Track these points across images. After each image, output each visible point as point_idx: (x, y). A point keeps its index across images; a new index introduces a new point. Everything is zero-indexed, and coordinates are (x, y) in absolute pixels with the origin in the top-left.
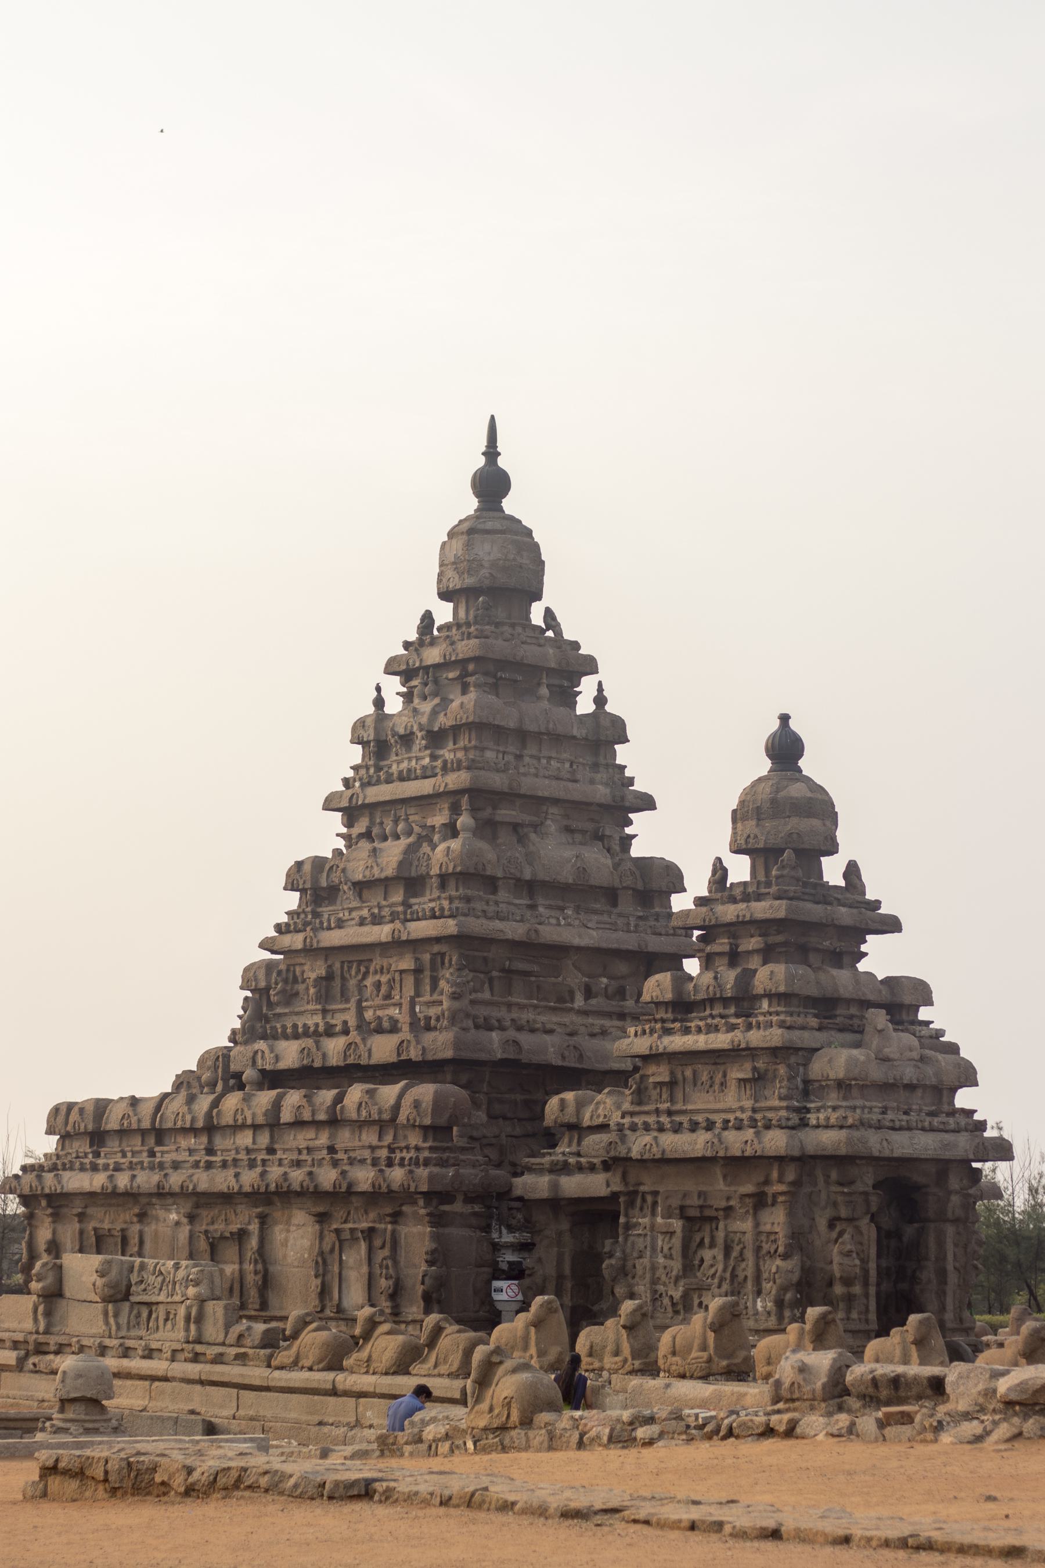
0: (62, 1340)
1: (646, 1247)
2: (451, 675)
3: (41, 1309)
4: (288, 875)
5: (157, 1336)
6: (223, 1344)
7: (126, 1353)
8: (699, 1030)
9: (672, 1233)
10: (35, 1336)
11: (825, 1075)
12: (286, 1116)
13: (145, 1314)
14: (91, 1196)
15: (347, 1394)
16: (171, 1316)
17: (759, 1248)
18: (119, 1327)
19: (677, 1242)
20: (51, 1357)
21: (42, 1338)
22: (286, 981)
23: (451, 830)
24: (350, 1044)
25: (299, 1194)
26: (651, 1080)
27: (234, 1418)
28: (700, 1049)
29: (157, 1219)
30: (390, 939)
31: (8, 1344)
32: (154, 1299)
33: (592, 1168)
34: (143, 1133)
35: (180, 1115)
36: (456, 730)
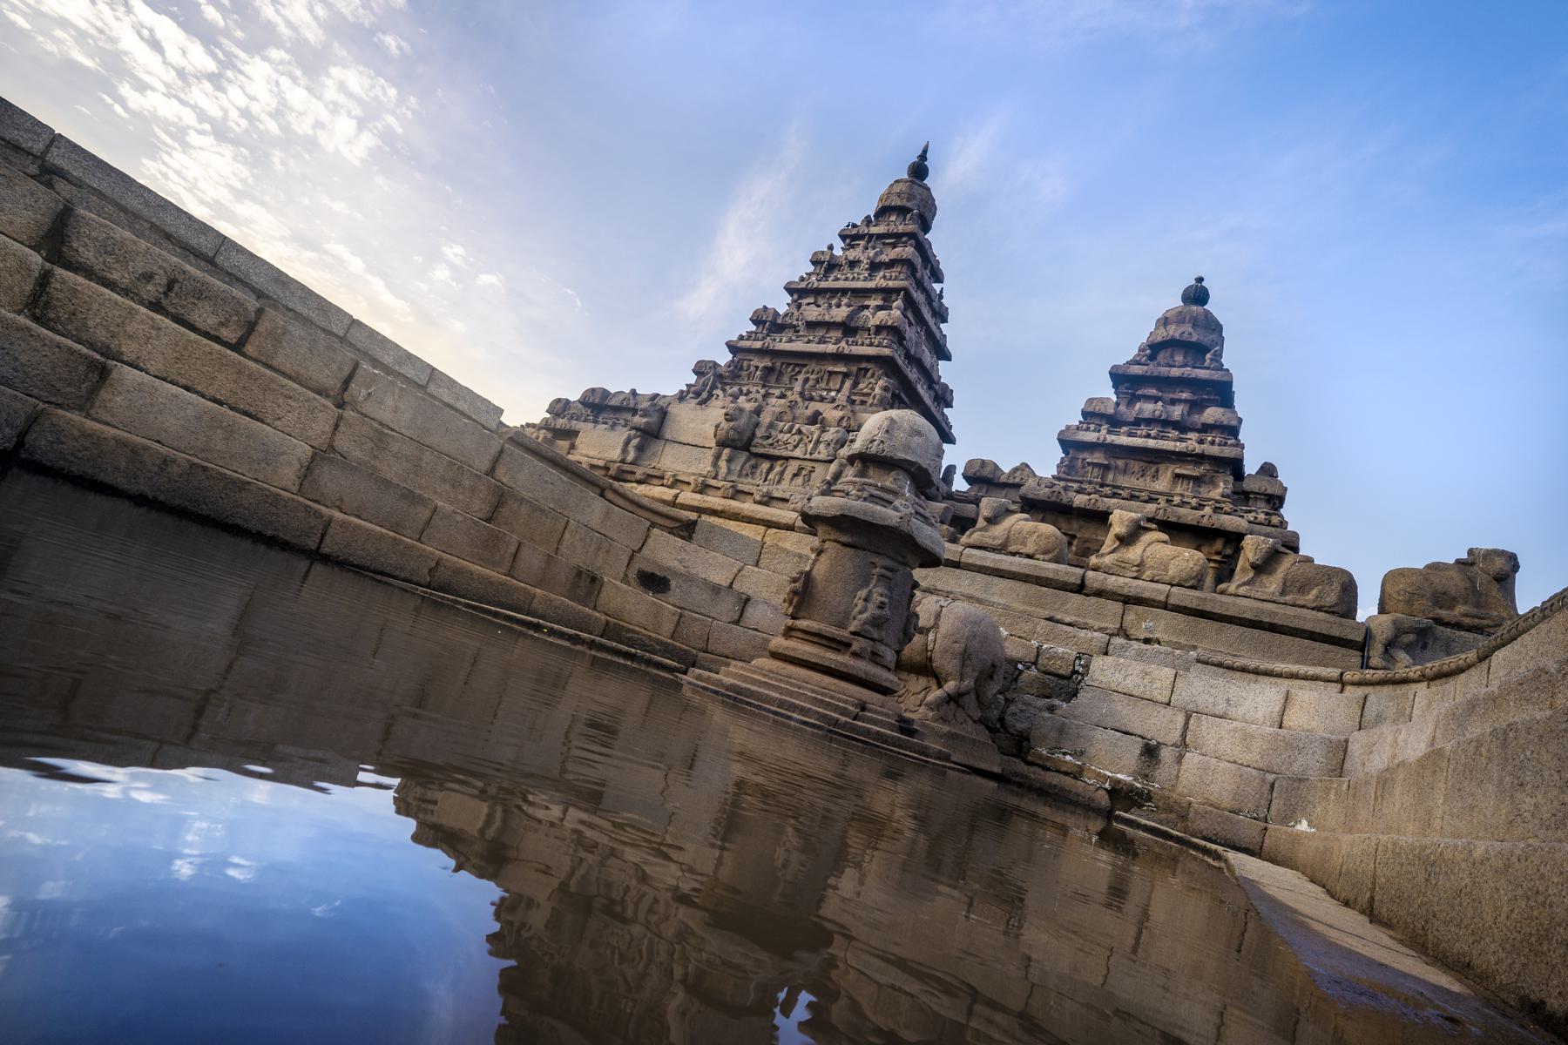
0: (651, 472)
2: (888, 241)
3: (635, 442)
4: (756, 312)
7: (737, 494)
13: (765, 465)
15: (1100, 593)
16: (804, 473)
18: (729, 472)
20: (634, 485)
21: (626, 467)
22: (736, 367)
23: (880, 308)
30: (835, 351)
32: (784, 453)
36: (891, 264)
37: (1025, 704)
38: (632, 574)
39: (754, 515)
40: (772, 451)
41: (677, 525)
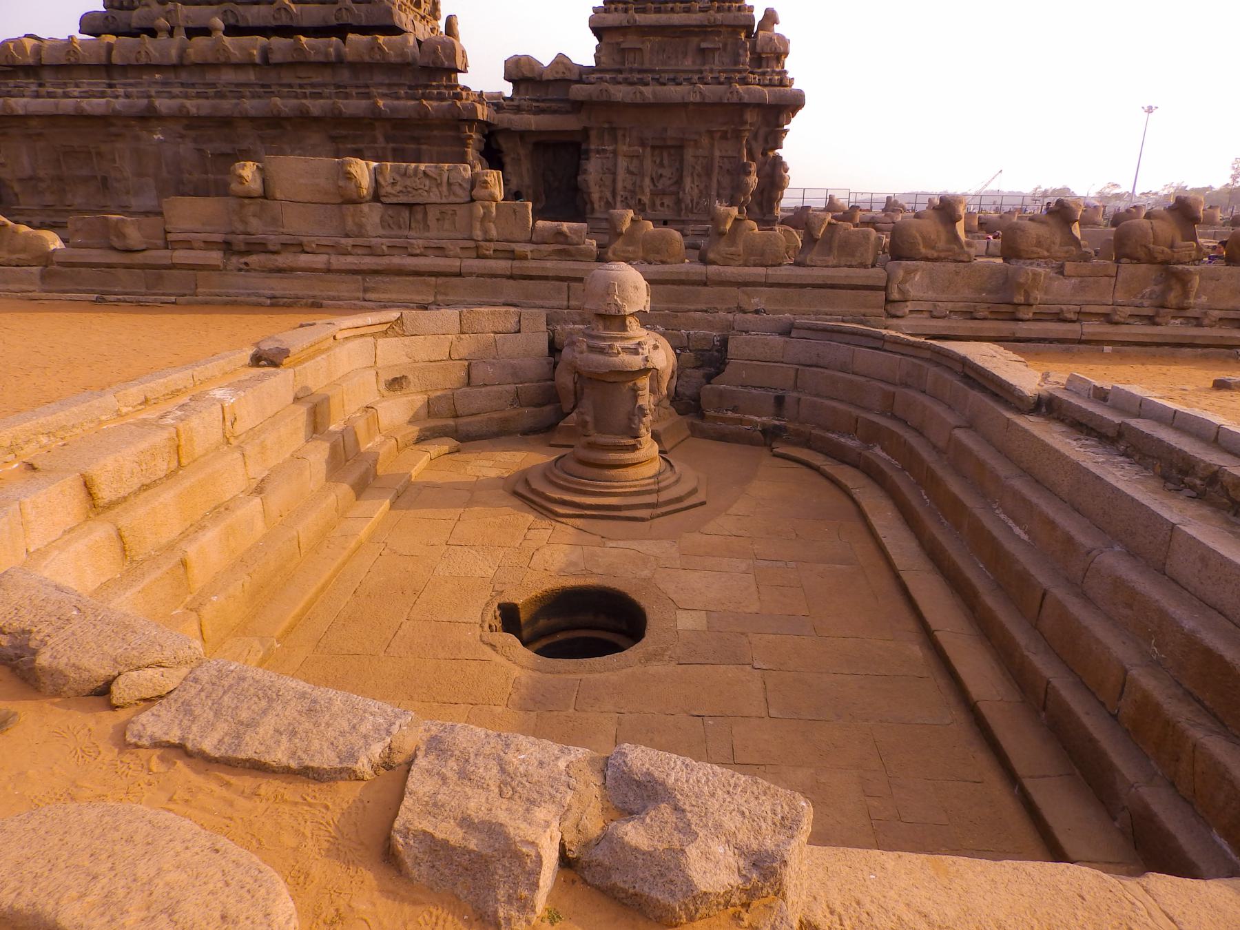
0: (284, 239)
1: (615, 165)
5: (427, 234)
6: (530, 241)
8: (672, 10)
9: (638, 156)
10: (241, 237)
11: (773, 49)
12: (276, 58)
13: (406, 213)
14: (53, 119)
17: (721, 167)
19: (648, 163)
21: (251, 238)
24: (279, 9)
25: (317, 119)
26: (623, 46)
27: (568, 308)
28: (675, 24)
29: (137, 138)
31: (196, 245)
33: (554, 112)
34: (92, 69)
35: (143, 53)
37: (687, 376)
38: (382, 387)
39: (417, 269)
40: (403, 199)
41: (389, 325)
